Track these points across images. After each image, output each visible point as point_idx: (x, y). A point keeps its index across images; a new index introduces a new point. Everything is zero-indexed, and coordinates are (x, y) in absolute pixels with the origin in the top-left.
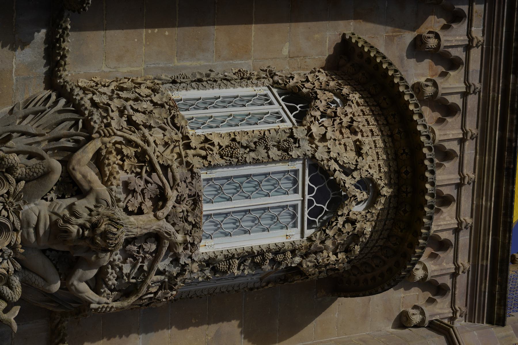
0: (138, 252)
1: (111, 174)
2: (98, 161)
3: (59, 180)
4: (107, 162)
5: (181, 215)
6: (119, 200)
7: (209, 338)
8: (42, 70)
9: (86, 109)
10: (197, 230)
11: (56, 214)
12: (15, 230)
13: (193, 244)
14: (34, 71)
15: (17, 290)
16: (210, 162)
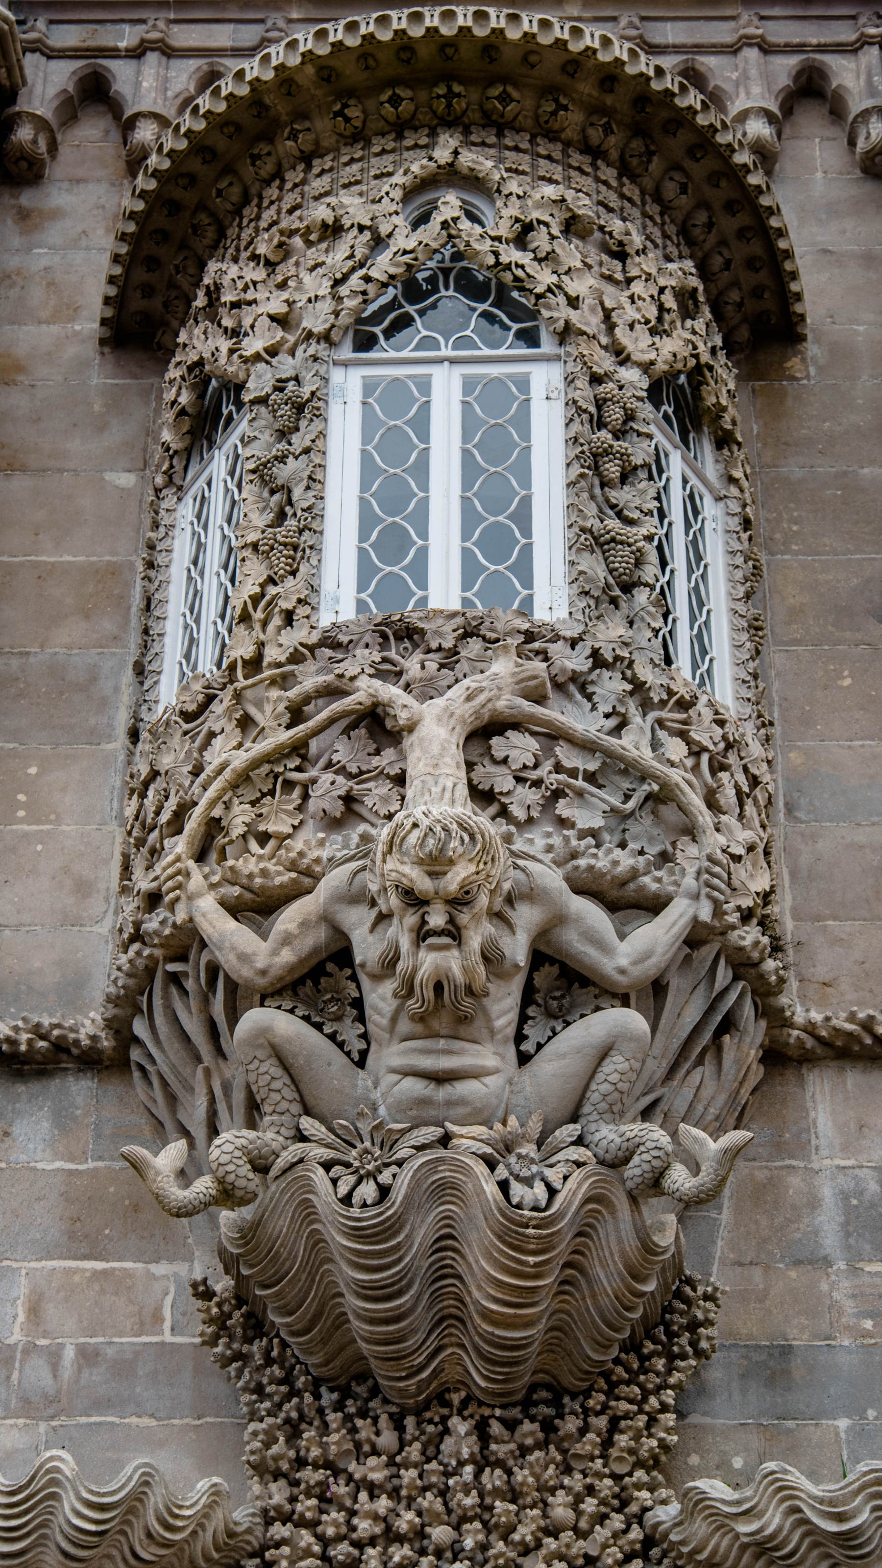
0: (537, 783)
1: (292, 866)
2: (257, 907)
3: (306, 1019)
4: (258, 881)
5: (432, 666)
6: (366, 838)
8: (80, 1089)
9: (138, 953)
10: (487, 623)
11: (394, 1020)
12: (445, 1140)
13: (530, 636)
14: (79, 1112)
15: (632, 1135)
16: (300, 601)
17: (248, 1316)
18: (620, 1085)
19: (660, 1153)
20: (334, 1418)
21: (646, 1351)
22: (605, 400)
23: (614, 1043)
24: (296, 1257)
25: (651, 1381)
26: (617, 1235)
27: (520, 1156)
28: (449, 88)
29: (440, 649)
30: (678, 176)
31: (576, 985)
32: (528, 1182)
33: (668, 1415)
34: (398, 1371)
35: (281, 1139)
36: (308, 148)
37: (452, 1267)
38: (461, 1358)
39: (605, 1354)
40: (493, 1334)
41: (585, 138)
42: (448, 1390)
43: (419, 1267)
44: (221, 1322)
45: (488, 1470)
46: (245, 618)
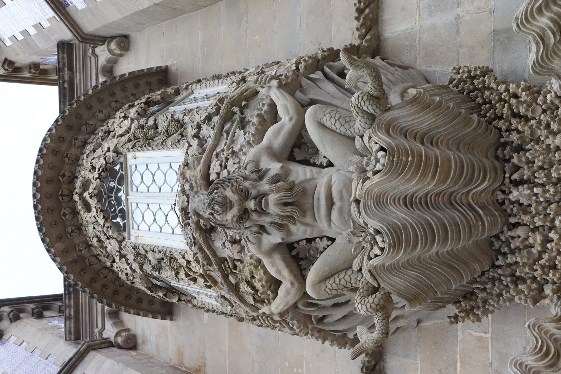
4: (264, 282)
7: (245, 19)
11: (306, 225)
17: (465, 297)
18: (336, 118)
19: (361, 96)
20: (510, 259)
21: (481, 101)
22: (135, 136)
23: (317, 122)
24: (417, 276)
25: (494, 97)
26: (406, 117)
27: (367, 165)
28: (60, 195)
29: (188, 202)
30: (97, 114)
31: (303, 140)
32: (378, 161)
33: (510, 88)
34: (478, 226)
35: (362, 279)
36: (85, 246)
37: (421, 198)
38: (476, 193)
39: (474, 121)
40: (452, 178)
41: (79, 147)
42: (497, 200)
43: (419, 216)
44: (469, 312)
45: (536, 180)
46: (195, 280)
